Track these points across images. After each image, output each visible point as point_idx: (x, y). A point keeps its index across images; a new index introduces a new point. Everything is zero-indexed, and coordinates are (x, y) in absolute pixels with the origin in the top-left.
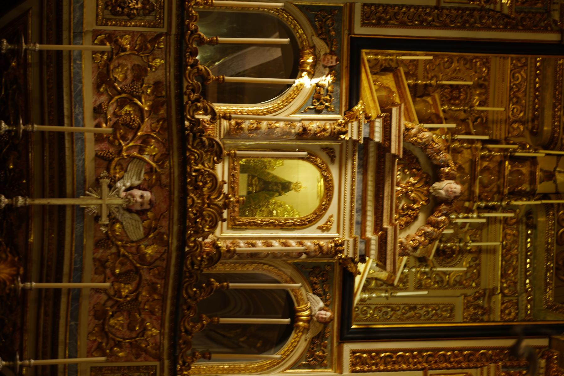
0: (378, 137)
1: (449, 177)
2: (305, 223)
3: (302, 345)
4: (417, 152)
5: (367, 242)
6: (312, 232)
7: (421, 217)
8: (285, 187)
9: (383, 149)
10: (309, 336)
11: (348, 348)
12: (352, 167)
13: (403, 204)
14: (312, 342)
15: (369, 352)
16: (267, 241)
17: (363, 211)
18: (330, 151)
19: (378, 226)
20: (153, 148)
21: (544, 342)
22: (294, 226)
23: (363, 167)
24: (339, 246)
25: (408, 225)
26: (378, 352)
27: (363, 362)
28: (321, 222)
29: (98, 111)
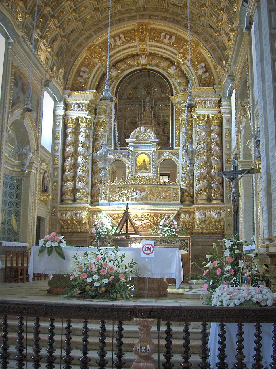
0: (132, 144)
1: (140, 129)
2: (150, 157)
3: (174, 157)
4: (136, 135)
5: (152, 146)
6: (151, 156)
7: (149, 134)
8: (144, 161)
9: (135, 143)
10: (172, 156)
11: (175, 148)
12: (139, 149)
13: (146, 138)
14: (173, 155)
15: (176, 143)
16: (153, 165)
17: (147, 146)
18: (136, 153)
19: (150, 143)
20: (129, 190)
21: (174, 107)
22: (150, 160)
23: (138, 146)
24: (154, 151)
25: (150, 137)
26: (176, 142)
27: (178, 144)
28: (150, 154)
29: (123, 200)
